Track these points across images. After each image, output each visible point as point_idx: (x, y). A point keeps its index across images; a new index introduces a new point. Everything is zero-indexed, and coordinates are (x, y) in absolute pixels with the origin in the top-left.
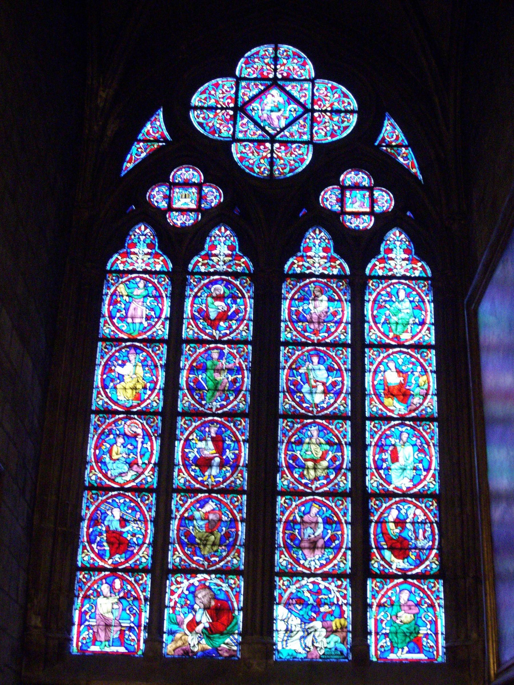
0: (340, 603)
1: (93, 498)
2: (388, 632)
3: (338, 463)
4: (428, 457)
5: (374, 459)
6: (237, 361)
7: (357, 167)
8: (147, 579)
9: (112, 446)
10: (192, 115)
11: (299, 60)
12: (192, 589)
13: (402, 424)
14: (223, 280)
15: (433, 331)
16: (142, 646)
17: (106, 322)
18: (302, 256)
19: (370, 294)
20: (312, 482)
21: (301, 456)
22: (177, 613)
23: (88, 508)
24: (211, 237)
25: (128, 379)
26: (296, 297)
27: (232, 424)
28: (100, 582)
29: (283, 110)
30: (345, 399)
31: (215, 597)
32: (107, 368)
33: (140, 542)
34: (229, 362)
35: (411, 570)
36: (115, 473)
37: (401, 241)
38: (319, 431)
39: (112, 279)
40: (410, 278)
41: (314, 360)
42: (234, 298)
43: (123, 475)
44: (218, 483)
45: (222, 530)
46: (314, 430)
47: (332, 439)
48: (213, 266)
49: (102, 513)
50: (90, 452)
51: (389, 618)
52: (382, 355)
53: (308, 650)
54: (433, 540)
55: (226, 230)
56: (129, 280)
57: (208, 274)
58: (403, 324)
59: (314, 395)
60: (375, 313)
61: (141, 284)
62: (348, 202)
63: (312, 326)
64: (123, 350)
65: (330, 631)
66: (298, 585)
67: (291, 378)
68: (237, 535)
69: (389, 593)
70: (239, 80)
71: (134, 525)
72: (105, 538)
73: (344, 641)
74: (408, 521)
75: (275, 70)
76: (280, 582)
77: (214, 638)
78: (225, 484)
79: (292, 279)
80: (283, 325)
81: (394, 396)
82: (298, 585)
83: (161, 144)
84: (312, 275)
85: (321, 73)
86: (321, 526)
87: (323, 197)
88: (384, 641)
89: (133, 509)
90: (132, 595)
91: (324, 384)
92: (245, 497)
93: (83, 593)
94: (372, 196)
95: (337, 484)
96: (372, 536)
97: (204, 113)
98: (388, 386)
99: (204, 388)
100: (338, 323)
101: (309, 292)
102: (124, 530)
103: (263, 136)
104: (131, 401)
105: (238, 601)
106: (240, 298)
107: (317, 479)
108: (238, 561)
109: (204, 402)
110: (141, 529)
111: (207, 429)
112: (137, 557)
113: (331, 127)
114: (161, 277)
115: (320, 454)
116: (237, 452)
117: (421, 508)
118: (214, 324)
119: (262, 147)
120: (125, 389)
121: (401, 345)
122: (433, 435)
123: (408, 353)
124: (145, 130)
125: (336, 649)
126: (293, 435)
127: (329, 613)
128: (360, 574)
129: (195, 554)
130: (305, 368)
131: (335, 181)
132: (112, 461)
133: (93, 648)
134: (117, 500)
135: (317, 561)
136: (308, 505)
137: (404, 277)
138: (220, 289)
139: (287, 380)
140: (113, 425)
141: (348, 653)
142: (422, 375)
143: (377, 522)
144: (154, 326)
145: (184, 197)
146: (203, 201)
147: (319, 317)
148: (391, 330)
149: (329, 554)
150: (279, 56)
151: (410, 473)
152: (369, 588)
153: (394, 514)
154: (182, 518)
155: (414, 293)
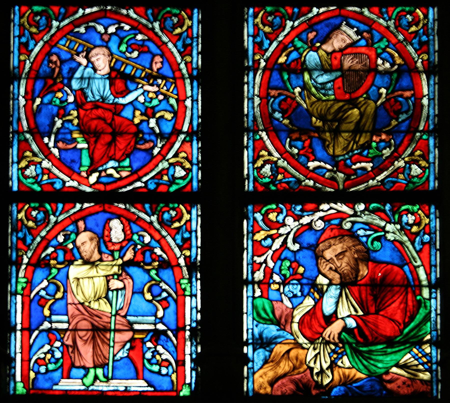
1: (37, 25)
8: (194, 217)
12: (309, 238)
16: (190, 376)
22: (273, 295)
23: (25, 48)
33: (167, 128)
71: (148, 88)
72: (76, 122)
77: (370, 352)
89: (142, 48)
92: (432, 13)
102: (122, 101)
134: (100, 29)
154: (272, 66)
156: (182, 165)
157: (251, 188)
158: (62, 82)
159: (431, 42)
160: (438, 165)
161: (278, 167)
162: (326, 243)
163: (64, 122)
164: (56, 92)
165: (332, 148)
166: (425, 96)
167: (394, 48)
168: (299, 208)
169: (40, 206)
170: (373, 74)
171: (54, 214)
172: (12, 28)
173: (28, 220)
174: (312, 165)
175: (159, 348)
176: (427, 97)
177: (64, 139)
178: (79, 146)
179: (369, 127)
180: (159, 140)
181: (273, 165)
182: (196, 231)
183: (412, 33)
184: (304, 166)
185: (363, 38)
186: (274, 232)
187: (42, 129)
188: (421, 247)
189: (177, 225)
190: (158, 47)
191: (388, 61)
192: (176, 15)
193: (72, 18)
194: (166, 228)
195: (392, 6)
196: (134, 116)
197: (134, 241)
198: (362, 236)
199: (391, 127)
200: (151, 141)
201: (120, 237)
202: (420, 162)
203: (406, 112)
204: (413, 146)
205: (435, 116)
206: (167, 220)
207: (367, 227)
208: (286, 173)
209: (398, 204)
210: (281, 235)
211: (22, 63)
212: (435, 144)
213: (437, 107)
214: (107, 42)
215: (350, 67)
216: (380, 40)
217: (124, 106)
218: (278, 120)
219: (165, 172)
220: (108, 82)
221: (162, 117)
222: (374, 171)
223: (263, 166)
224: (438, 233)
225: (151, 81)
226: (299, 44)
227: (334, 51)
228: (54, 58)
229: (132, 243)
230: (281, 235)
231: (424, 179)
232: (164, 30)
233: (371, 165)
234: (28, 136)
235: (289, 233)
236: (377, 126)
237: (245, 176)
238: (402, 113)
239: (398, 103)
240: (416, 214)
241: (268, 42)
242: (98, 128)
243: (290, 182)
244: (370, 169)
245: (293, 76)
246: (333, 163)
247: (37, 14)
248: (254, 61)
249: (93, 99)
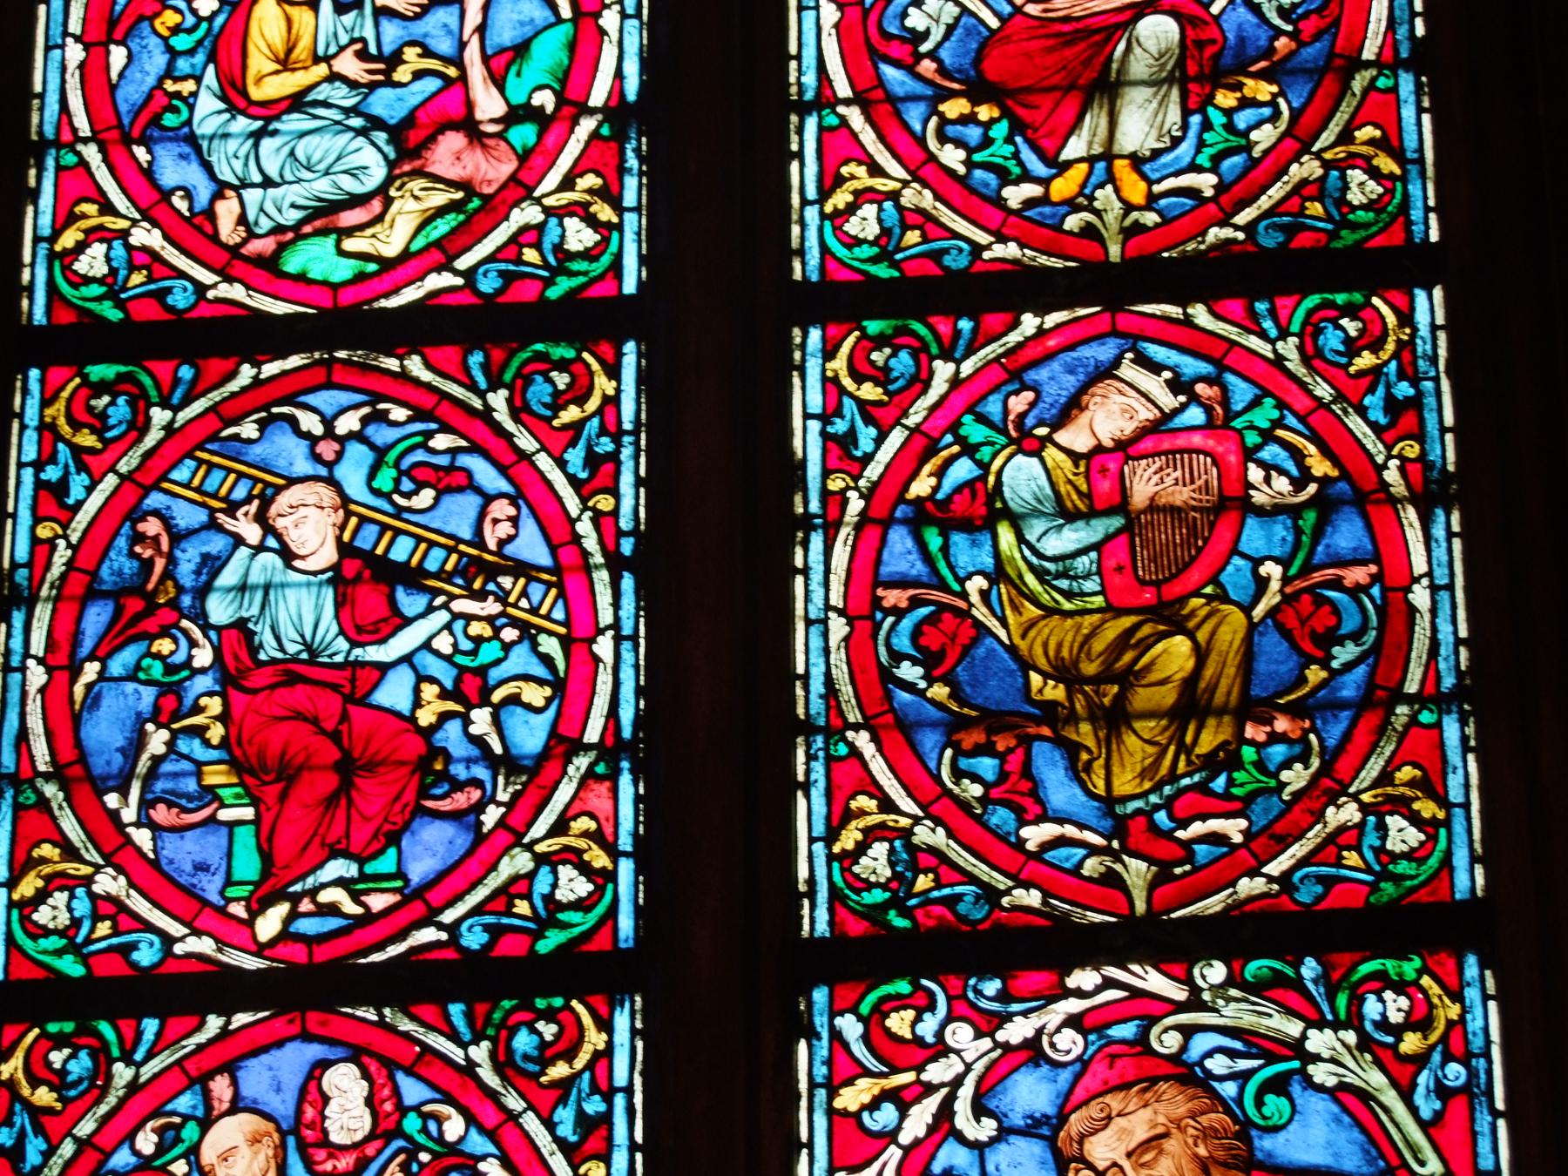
8: (621, 1038)
23: (54, 501)
33: (530, 735)
36: (285, 204)
43: (349, 218)
45: (1262, 584)
71: (463, 605)
72: (216, 733)
78: (1242, 218)
92: (1429, 306)
102: (373, 653)
110: (523, 626)
132: (243, 124)
156: (584, 865)
157: (822, 928)
158: (174, 604)
159: (1430, 401)
160: (1482, 812)
161: (911, 848)
162: (1094, 1110)
163: (175, 734)
164: (152, 638)
165: (1102, 773)
166: (1417, 580)
167: (1300, 427)
168: (992, 987)
169: (78, 1032)
170: (1232, 517)
171: (127, 1059)
172: (14, 440)
173: (35, 1084)
174: (1034, 835)
176: (1425, 582)
177: (172, 792)
178: (225, 815)
179: (1229, 693)
180: (501, 780)
181: (897, 843)
182: (629, 1090)
183: (1361, 373)
184: (1003, 839)
185: (1194, 398)
186: (908, 1077)
187: (98, 765)
188: (1438, 1105)
189: (559, 1070)
190: (503, 470)
191: (1282, 472)
192: (563, 365)
193: (216, 396)
194: (521, 1082)
195: (1287, 292)
196: (417, 703)
197: (409, 1139)
198: (1222, 1079)
199: (1306, 690)
200: (477, 783)
201: (353, 1124)
202: (1416, 806)
203: (1356, 637)
204: (1387, 753)
205: (1458, 642)
206: (526, 1057)
207: (1238, 1045)
208: (943, 869)
209: (1345, 958)
210: (930, 1089)
211: (42, 549)
212: (1464, 739)
213: (1461, 614)
214: (330, 465)
215: (1152, 499)
216: (1255, 403)
217: (383, 668)
218: (909, 687)
219: (521, 887)
220: (329, 594)
221: (514, 700)
222: (1253, 846)
223: (862, 848)
224: (1496, 1052)
225: (477, 585)
226: (974, 432)
227: (1099, 449)
228: (152, 527)
229: (399, 1143)
230: (930, 1089)
231: (1433, 862)
232: (524, 416)
233: (1243, 823)
234: (50, 790)
235: (958, 1082)
236: (1256, 691)
237: (802, 888)
238: (1340, 642)
239: (1327, 608)
240: (1411, 990)
241: (873, 432)
242: (291, 752)
243: (959, 898)
244: (1238, 838)
245: (959, 539)
246: (1107, 824)
247: (101, 388)
248: (825, 494)
249: (280, 655)
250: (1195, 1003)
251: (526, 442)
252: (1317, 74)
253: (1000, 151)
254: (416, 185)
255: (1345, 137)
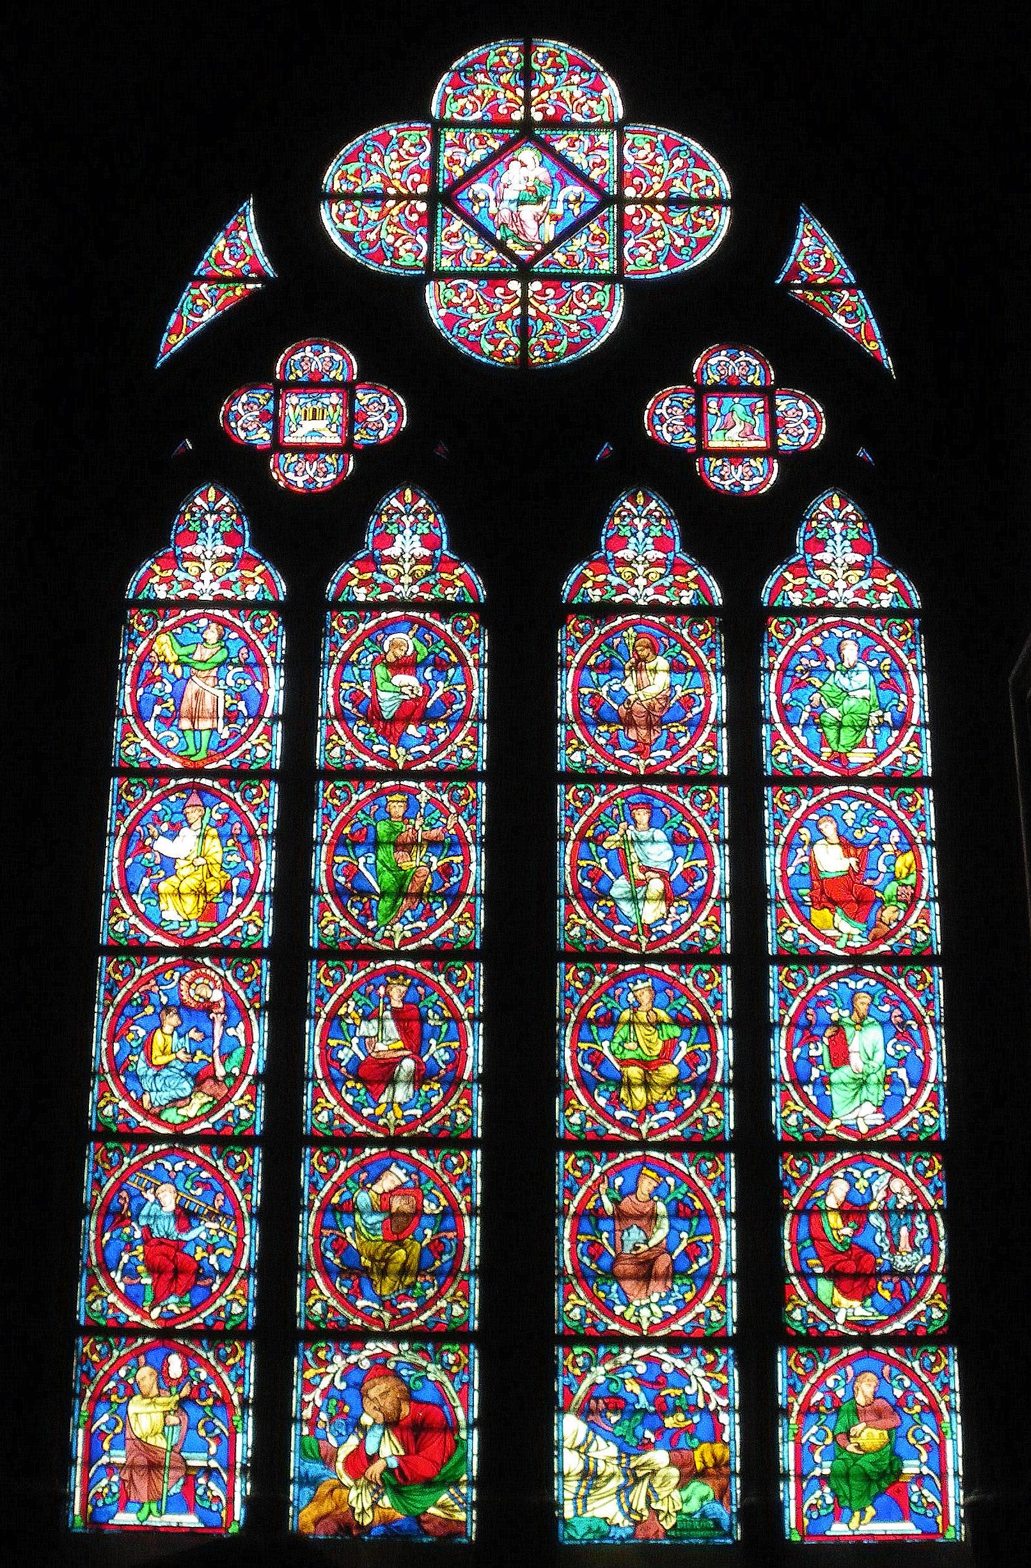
0: (712, 1407)
2: (827, 1472)
3: (701, 1069)
4: (919, 1052)
5: (789, 1058)
6: (451, 823)
7: (735, 340)
9: (151, 1034)
10: (327, 215)
11: (586, 76)
12: (356, 1377)
13: (856, 972)
14: (413, 621)
15: (927, 745)
16: (239, 1513)
17: (127, 728)
18: (604, 560)
19: (773, 651)
20: (641, 1116)
21: (614, 1054)
22: (320, 1434)
23: (98, 1184)
24: (380, 516)
25: (184, 868)
26: (592, 661)
27: (442, 977)
28: (133, 1362)
29: (548, 199)
30: (715, 911)
31: (409, 1396)
32: (135, 843)
33: (227, 1267)
34: (429, 824)
35: (880, 1324)
36: (162, 1098)
37: (845, 520)
38: (654, 991)
39: (139, 623)
40: (868, 613)
41: (637, 818)
42: (440, 666)
43: (181, 1103)
44: (413, 1121)
46: (642, 989)
47: (685, 1012)
48: (386, 587)
49: (131, 1198)
50: (99, 1048)
51: (829, 1441)
52: (805, 804)
53: (637, 1518)
54: (935, 1253)
55: (416, 497)
56: (180, 624)
57: (375, 607)
58: (854, 727)
59: (641, 905)
60: (786, 697)
61: (212, 635)
62: (713, 422)
63: (632, 734)
64: (172, 798)
65: (689, 1475)
66: (609, 1366)
67: (583, 863)
68: (461, 1247)
69: (830, 1382)
70: (438, 126)
71: (209, 1225)
72: (141, 1257)
73: (722, 1495)
74: (873, 1206)
75: (527, 101)
76: (571, 1359)
78: (428, 1124)
79: (582, 617)
80: (561, 730)
81: (836, 903)
82: (609, 1366)
83: (250, 286)
84: (628, 607)
85: (642, 107)
86: (665, 1222)
87: (652, 414)
88: (818, 1493)
89: (205, 1184)
90: (210, 1394)
91: (664, 875)
92: (477, 1155)
93: (92, 1388)
94: (771, 408)
95: (702, 1121)
96: (787, 1246)
97: (355, 209)
98: (821, 881)
99: (369, 892)
100: (699, 724)
101: (623, 651)
103: (501, 263)
104: (193, 923)
105: (467, 1408)
106: (455, 666)
107: (651, 1108)
108: (464, 1309)
109: (371, 924)
111: (382, 991)
112: (221, 1301)
113: (667, 240)
114: (259, 616)
115: (658, 1048)
116: (456, 1045)
117: (904, 1176)
118: (391, 729)
119: (499, 291)
120: (180, 894)
121: (850, 778)
122: (930, 997)
123: (866, 798)
124: (213, 251)
125: (704, 1515)
126: (591, 1002)
127: (686, 1430)
128: (760, 1338)
129: (359, 1293)
130: (617, 837)
131: (680, 373)
132: (151, 1072)
133: (124, 1518)
134: (168, 1166)
135: (654, 1307)
136: (631, 1172)
137: (854, 610)
138: (403, 642)
139: (575, 868)
140: (153, 982)
141: (731, 1525)
142: (903, 853)
143: (798, 1212)
144: (246, 737)
145: (313, 418)
146: (357, 427)
147: (650, 709)
148: (824, 742)
149: (683, 1291)
150: (536, 66)
151: (876, 1093)
152: (781, 1369)
153: (839, 1190)
155: (880, 648)
174: (360, 1304)
175: (211, 1485)
226: (350, 1184)
250: (400, 1354)
251: (227, 1177)
252: (450, 1084)
253: (362, 1098)
254: (200, 1095)
255: (457, 1102)
